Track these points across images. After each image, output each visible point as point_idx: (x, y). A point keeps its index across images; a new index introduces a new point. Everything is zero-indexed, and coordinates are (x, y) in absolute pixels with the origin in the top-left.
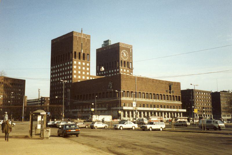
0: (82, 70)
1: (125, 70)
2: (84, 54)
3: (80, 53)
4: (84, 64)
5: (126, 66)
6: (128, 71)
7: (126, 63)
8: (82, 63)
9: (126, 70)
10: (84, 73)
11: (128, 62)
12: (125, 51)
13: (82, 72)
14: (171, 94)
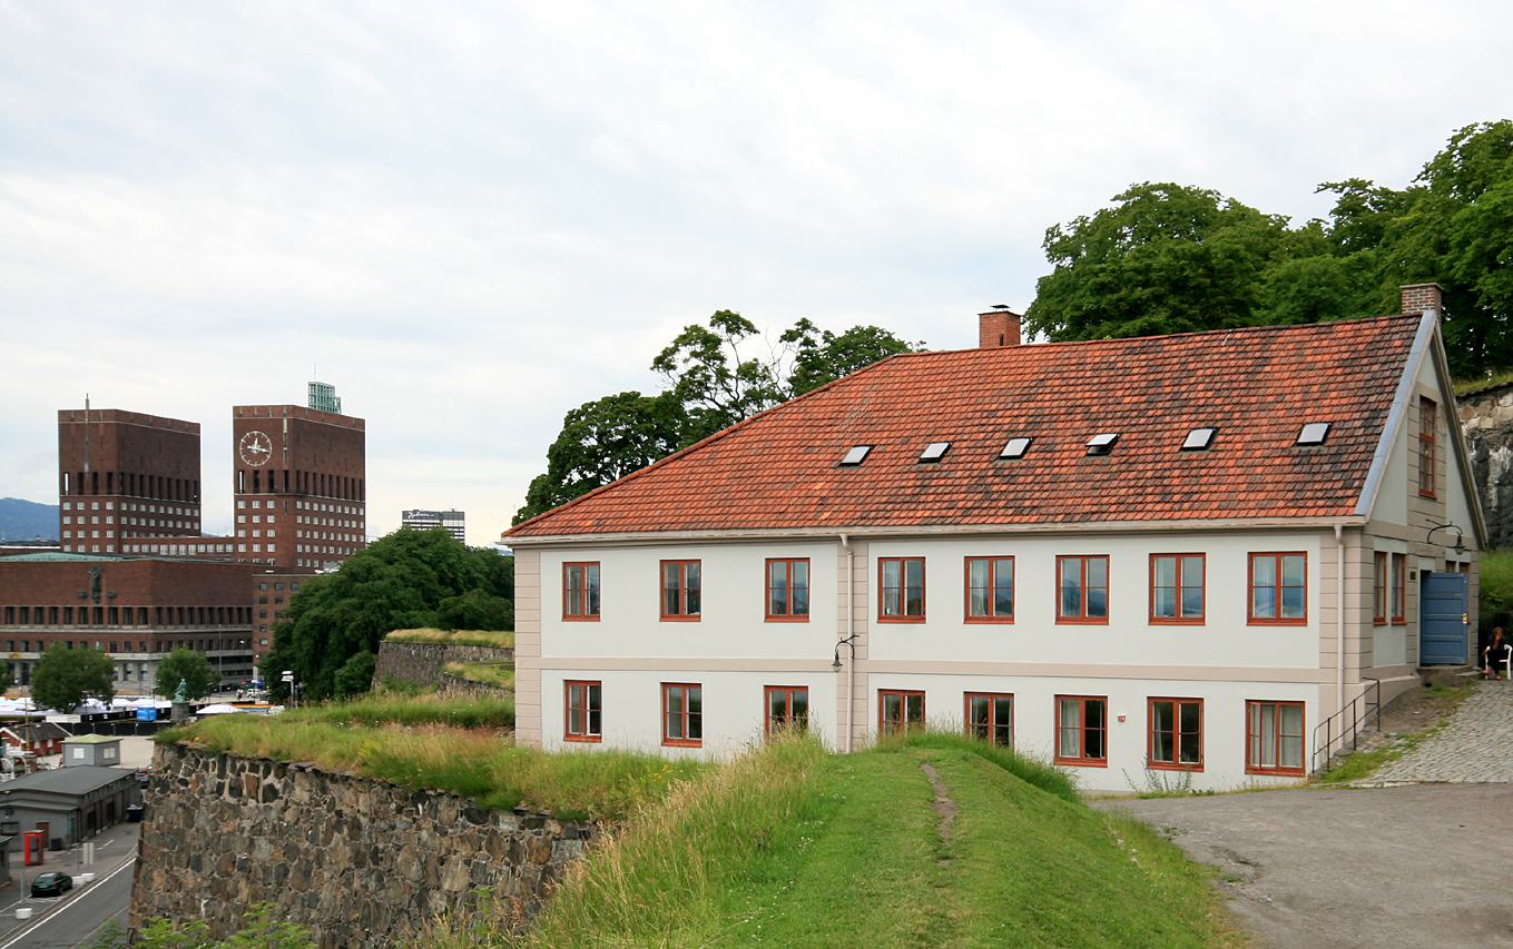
0: (88, 528)
1: (256, 505)
2: (95, 475)
3: (81, 475)
4: (95, 506)
5: (264, 486)
6: (271, 505)
7: (263, 478)
8: (88, 506)
9: (264, 504)
10: (95, 535)
11: (271, 472)
12: (256, 432)
13: (89, 534)
14: (104, 604)
